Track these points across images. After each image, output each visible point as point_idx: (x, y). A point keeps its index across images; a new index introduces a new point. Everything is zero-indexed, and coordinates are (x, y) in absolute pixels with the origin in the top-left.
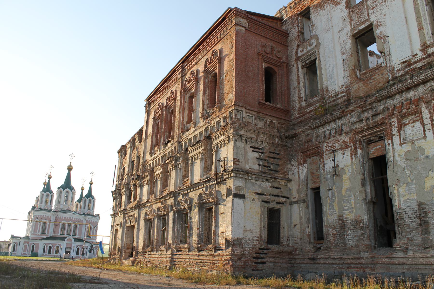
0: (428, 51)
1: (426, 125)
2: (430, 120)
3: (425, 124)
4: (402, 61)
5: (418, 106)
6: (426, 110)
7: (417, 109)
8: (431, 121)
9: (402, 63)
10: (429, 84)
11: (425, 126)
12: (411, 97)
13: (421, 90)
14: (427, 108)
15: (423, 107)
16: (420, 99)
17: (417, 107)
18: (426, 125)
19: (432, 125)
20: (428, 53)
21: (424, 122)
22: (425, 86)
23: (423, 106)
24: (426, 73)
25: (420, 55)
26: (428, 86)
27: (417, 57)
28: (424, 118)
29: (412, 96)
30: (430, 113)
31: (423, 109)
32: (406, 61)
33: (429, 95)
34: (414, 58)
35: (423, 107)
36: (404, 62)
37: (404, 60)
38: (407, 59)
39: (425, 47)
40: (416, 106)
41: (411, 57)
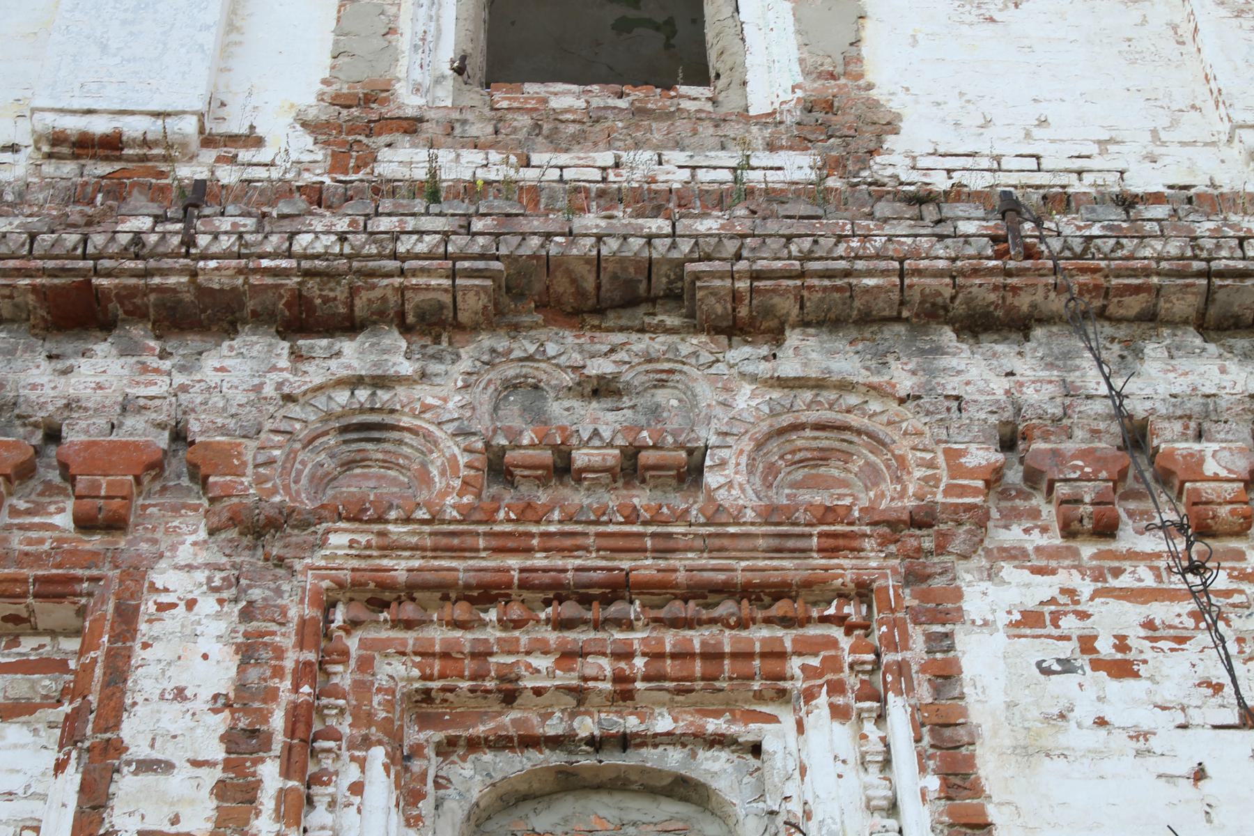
0: (384, 154)
1: (146, 766)
2: (220, 722)
3: (139, 749)
4: (73, 125)
5: (116, 525)
6: (208, 605)
7: (93, 559)
8: (229, 739)
9: (57, 139)
10: (352, 354)
11: (126, 785)
12: (70, 405)
13: (234, 376)
14: (231, 586)
15: (183, 561)
16: (182, 461)
17: (95, 542)
18: (146, 766)
19: (221, 790)
20: (380, 169)
21: (135, 732)
22: (297, 356)
23: (185, 554)
24: (385, 224)
25: (289, 150)
26: (337, 368)
27: (244, 155)
28: (146, 679)
29: (93, 399)
30: (247, 652)
31: (164, 576)
32: (111, 145)
33: (309, 461)
34: (209, 155)
35: (183, 561)
36: (84, 146)
37: (100, 126)
38: (133, 127)
39: (358, 117)
40: (85, 524)
41: (189, 126)
